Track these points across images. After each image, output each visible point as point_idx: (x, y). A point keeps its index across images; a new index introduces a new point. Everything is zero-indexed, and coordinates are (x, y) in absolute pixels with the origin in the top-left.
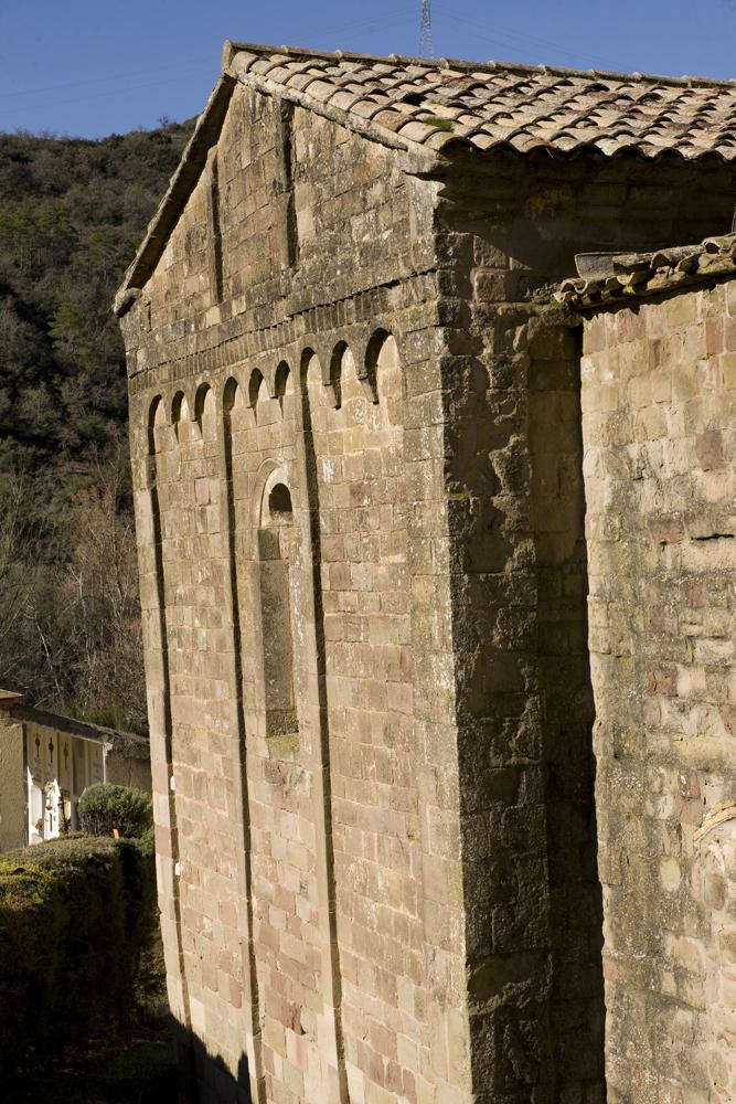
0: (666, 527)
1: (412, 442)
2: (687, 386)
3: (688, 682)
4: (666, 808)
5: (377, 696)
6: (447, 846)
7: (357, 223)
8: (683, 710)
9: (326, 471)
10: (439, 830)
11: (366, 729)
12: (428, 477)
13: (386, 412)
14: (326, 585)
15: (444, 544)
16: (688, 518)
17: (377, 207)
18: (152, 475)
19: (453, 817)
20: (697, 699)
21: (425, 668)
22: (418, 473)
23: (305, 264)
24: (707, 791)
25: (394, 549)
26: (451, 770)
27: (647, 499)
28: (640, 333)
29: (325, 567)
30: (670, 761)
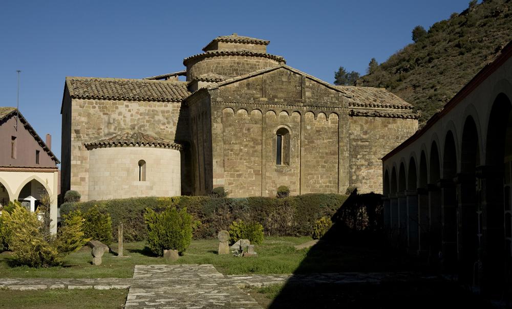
0: (355, 140)
2: (362, 126)
3: (359, 157)
4: (353, 170)
5: (322, 157)
6: (346, 174)
8: (358, 159)
11: (318, 162)
12: (344, 131)
13: (330, 123)
16: (361, 139)
17: (332, 97)
20: (361, 158)
21: (342, 153)
24: (362, 168)
27: (352, 137)
28: (353, 119)
30: (355, 165)
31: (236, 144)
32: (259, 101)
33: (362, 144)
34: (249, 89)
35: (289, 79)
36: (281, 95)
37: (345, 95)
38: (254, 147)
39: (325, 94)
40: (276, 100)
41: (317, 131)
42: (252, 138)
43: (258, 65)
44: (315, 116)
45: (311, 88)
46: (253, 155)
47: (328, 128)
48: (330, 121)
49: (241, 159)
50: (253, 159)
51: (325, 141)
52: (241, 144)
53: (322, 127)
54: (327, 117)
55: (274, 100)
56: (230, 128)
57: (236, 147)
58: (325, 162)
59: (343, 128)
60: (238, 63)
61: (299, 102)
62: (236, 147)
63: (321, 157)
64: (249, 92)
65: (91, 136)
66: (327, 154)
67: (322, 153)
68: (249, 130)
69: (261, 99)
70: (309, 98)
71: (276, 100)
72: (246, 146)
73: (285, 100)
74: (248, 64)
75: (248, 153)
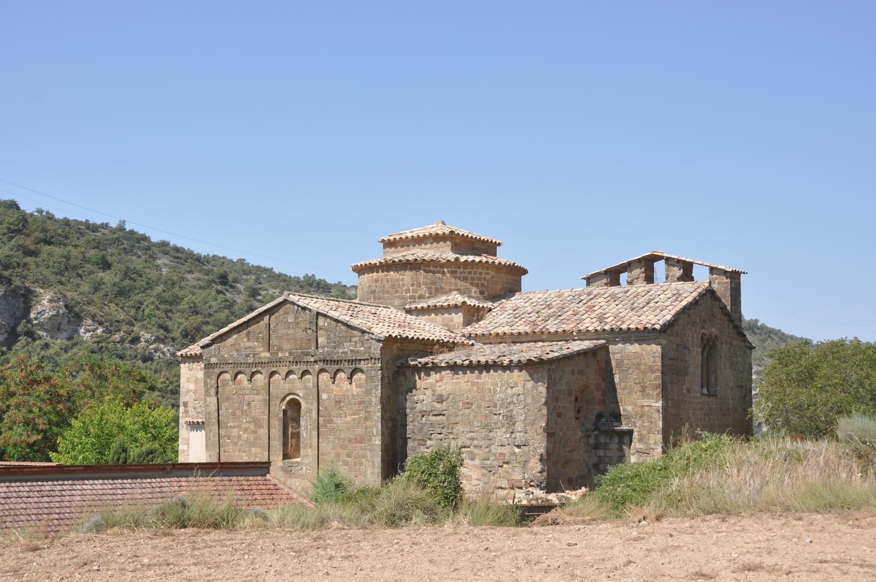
1: (368, 392)
7: (346, 344)
9: (324, 396)
10: (373, 473)
11: (338, 455)
12: (374, 399)
14: (321, 422)
15: (379, 414)
18: (217, 393)
19: (380, 470)
21: (370, 440)
22: (371, 400)
23: (320, 350)
25: (355, 414)
26: (379, 460)
29: (320, 418)
31: (234, 427)
32: (260, 358)
33: (434, 418)
34: (249, 340)
35: (296, 318)
36: (286, 346)
37: (373, 337)
38: (255, 432)
39: (346, 337)
40: (280, 355)
41: (336, 402)
42: (253, 418)
43: (403, 280)
44: (334, 378)
45: (327, 330)
46: (254, 445)
47: (353, 395)
48: (354, 383)
49: (239, 451)
50: (254, 450)
51: (348, 419)
52: (239, 427)
53: (344, 396)
54: (350, 378)
55: (277, 354)
56: (227, 404)
57: (235, 432)
58: (349, 456)
59: (371, 394)
60: (377, 281)
61: (308, 354)
62: (235, 432)
63: (342, 447)
64: (248, 344)
65: (199, 410)
66: (350, 440)
67: (344, 440)
68: (249, 404)
69: (263, 355)
70: (323, 347)
71: (280, 355)
72: (246, 430)
73: (290, 353)
74: (388, 281)
75: (247, 441)
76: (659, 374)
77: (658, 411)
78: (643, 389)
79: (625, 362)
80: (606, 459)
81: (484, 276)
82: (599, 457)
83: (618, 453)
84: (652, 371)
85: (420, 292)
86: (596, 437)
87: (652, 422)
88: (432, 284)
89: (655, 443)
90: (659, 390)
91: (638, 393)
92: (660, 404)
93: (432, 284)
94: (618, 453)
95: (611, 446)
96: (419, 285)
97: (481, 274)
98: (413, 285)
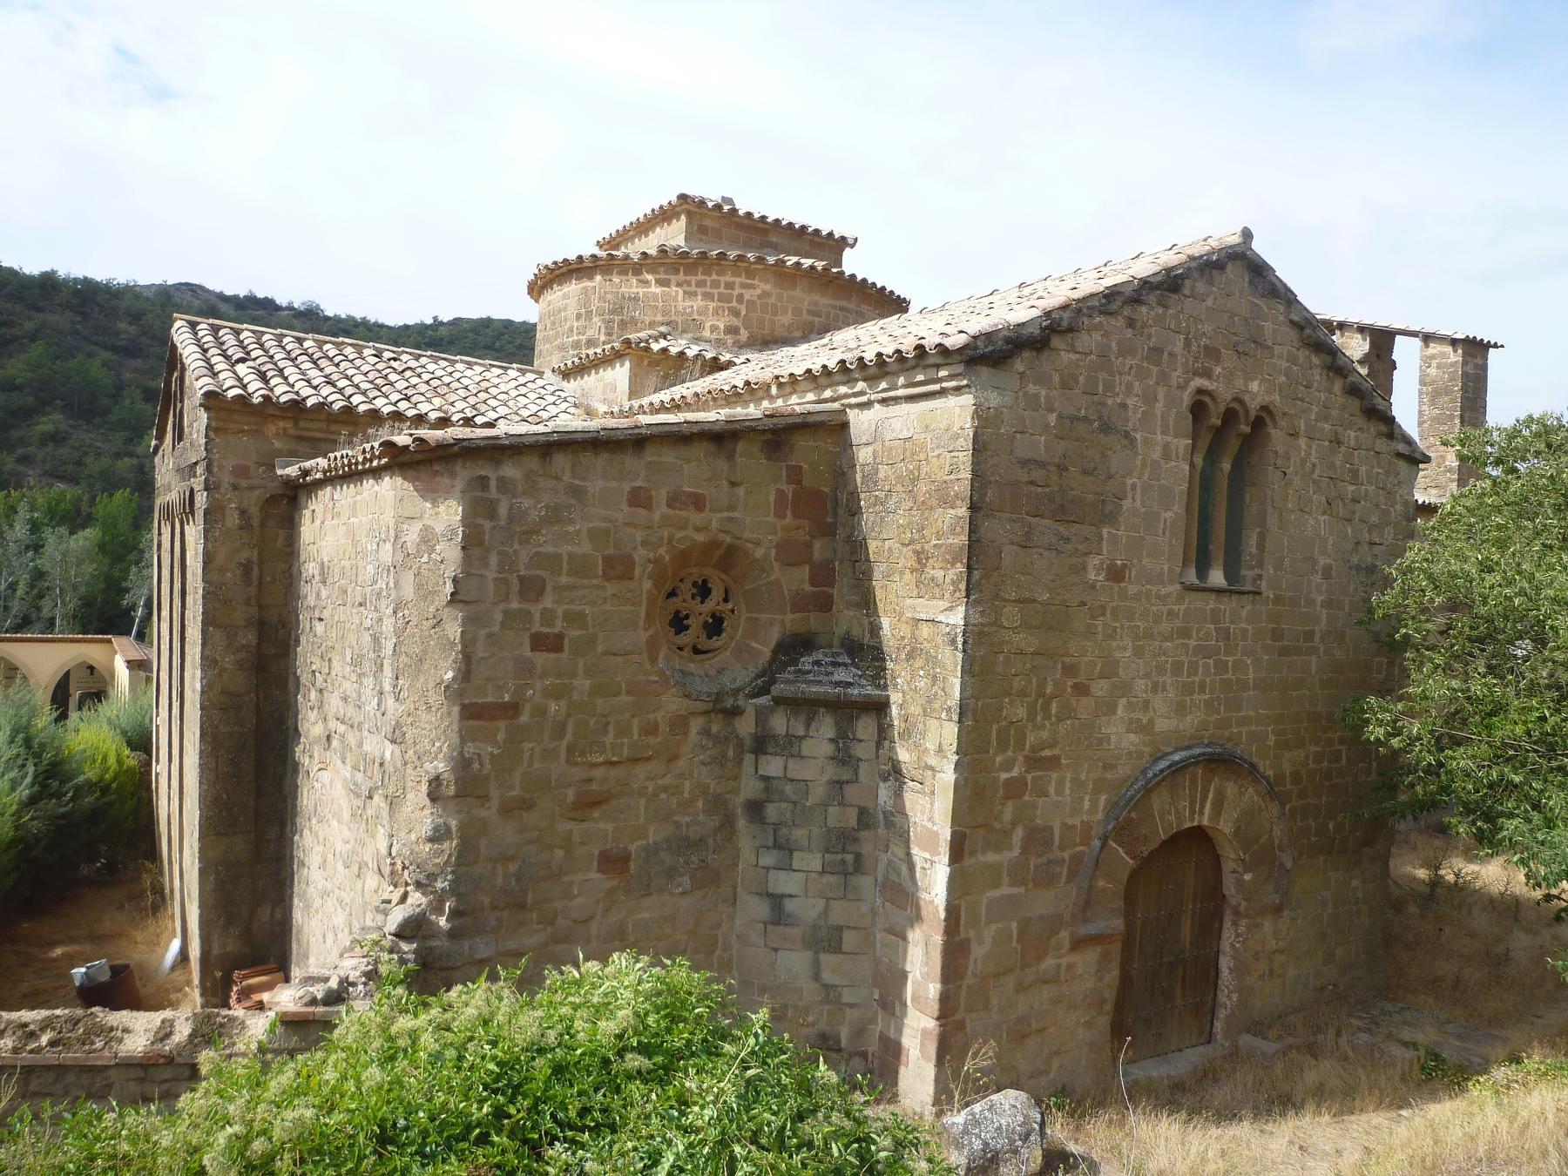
76: (963, 511)
77: (953, 642)
78: (921, 558)
79: (883, 471)
80: (788, 788)
81: (736, 292)
82: (766, 779)
83: (831, 772)
84: (947, 502)
85: (590, 333)
86: (761, 716)
87: (935, 678)
88: (612, 312)
89: (940, 750)
90: (960, 568)
91: (907, 576)
92: (957, 617)
93: (612, 312)
94: (831, 772)
95: (807, 747)
96: (589, 314)
97: (730, 286)
98: (579, 317)
